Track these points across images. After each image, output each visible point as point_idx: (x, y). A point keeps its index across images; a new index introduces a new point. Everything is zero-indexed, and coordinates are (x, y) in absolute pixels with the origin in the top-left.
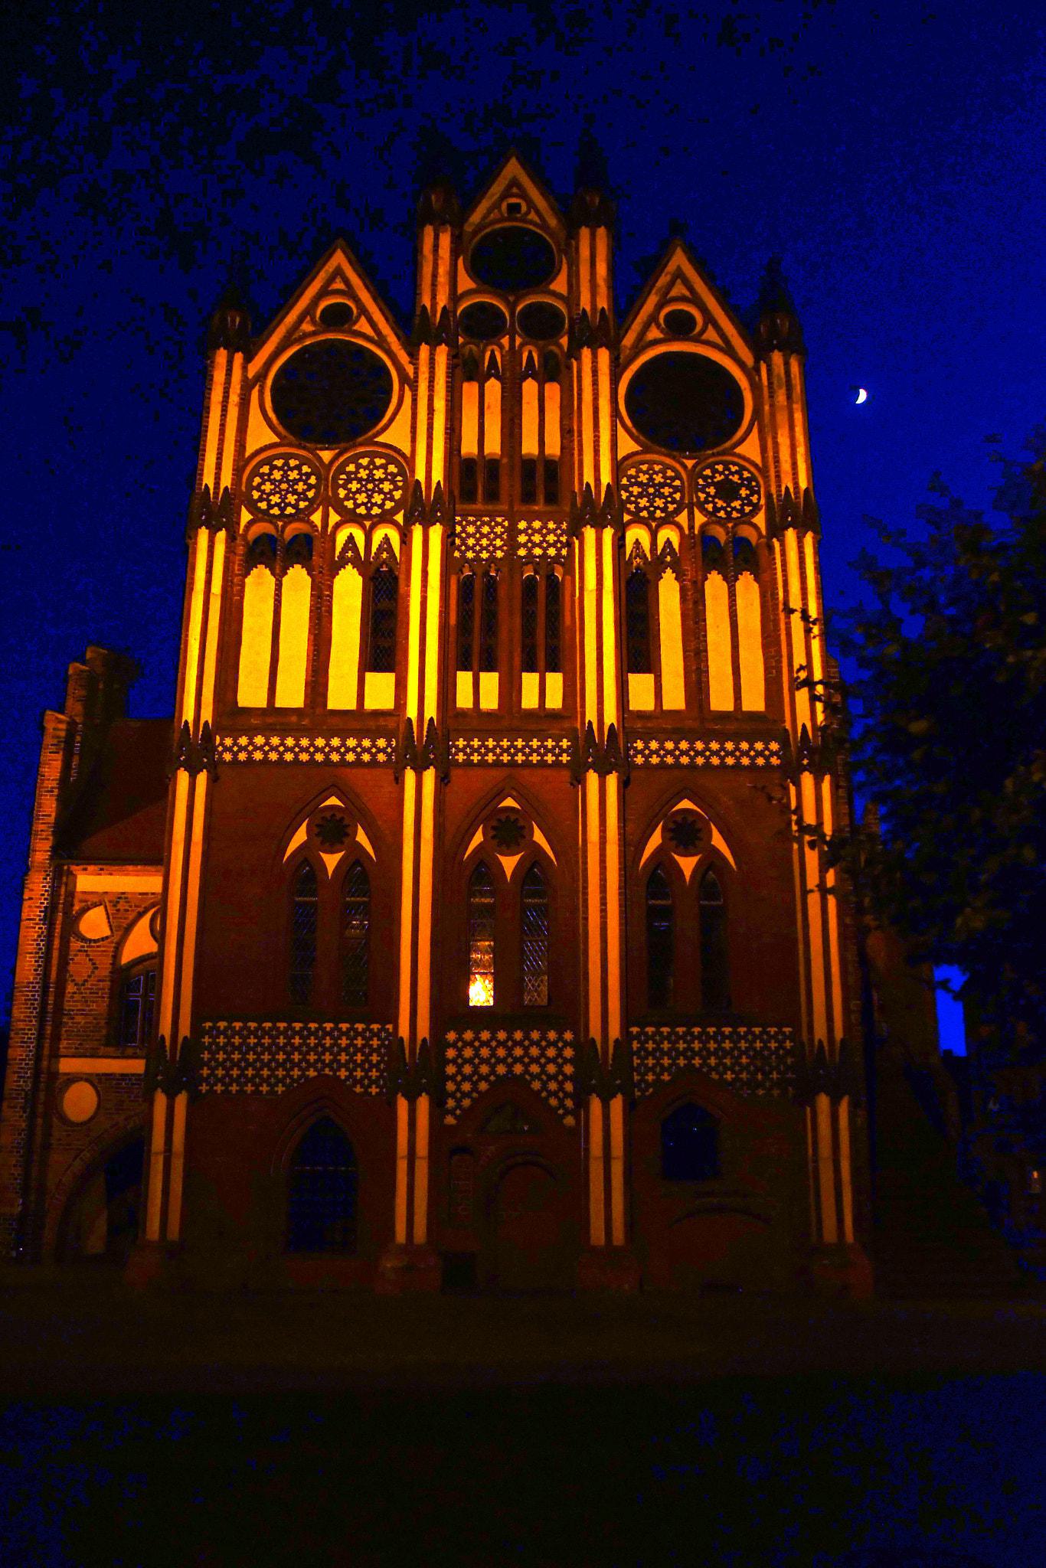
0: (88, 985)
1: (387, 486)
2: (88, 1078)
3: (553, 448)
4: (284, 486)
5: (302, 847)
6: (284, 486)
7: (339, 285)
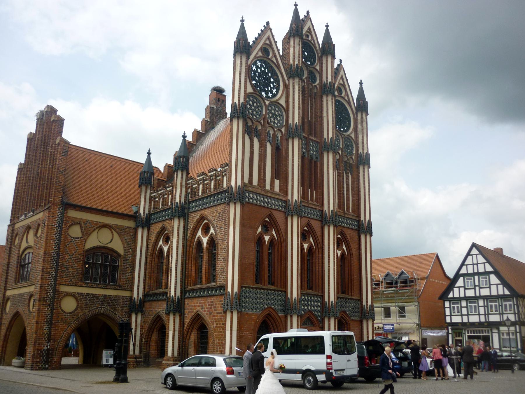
0: (74, 256)
5: (260, 233)
6: (253, 108)
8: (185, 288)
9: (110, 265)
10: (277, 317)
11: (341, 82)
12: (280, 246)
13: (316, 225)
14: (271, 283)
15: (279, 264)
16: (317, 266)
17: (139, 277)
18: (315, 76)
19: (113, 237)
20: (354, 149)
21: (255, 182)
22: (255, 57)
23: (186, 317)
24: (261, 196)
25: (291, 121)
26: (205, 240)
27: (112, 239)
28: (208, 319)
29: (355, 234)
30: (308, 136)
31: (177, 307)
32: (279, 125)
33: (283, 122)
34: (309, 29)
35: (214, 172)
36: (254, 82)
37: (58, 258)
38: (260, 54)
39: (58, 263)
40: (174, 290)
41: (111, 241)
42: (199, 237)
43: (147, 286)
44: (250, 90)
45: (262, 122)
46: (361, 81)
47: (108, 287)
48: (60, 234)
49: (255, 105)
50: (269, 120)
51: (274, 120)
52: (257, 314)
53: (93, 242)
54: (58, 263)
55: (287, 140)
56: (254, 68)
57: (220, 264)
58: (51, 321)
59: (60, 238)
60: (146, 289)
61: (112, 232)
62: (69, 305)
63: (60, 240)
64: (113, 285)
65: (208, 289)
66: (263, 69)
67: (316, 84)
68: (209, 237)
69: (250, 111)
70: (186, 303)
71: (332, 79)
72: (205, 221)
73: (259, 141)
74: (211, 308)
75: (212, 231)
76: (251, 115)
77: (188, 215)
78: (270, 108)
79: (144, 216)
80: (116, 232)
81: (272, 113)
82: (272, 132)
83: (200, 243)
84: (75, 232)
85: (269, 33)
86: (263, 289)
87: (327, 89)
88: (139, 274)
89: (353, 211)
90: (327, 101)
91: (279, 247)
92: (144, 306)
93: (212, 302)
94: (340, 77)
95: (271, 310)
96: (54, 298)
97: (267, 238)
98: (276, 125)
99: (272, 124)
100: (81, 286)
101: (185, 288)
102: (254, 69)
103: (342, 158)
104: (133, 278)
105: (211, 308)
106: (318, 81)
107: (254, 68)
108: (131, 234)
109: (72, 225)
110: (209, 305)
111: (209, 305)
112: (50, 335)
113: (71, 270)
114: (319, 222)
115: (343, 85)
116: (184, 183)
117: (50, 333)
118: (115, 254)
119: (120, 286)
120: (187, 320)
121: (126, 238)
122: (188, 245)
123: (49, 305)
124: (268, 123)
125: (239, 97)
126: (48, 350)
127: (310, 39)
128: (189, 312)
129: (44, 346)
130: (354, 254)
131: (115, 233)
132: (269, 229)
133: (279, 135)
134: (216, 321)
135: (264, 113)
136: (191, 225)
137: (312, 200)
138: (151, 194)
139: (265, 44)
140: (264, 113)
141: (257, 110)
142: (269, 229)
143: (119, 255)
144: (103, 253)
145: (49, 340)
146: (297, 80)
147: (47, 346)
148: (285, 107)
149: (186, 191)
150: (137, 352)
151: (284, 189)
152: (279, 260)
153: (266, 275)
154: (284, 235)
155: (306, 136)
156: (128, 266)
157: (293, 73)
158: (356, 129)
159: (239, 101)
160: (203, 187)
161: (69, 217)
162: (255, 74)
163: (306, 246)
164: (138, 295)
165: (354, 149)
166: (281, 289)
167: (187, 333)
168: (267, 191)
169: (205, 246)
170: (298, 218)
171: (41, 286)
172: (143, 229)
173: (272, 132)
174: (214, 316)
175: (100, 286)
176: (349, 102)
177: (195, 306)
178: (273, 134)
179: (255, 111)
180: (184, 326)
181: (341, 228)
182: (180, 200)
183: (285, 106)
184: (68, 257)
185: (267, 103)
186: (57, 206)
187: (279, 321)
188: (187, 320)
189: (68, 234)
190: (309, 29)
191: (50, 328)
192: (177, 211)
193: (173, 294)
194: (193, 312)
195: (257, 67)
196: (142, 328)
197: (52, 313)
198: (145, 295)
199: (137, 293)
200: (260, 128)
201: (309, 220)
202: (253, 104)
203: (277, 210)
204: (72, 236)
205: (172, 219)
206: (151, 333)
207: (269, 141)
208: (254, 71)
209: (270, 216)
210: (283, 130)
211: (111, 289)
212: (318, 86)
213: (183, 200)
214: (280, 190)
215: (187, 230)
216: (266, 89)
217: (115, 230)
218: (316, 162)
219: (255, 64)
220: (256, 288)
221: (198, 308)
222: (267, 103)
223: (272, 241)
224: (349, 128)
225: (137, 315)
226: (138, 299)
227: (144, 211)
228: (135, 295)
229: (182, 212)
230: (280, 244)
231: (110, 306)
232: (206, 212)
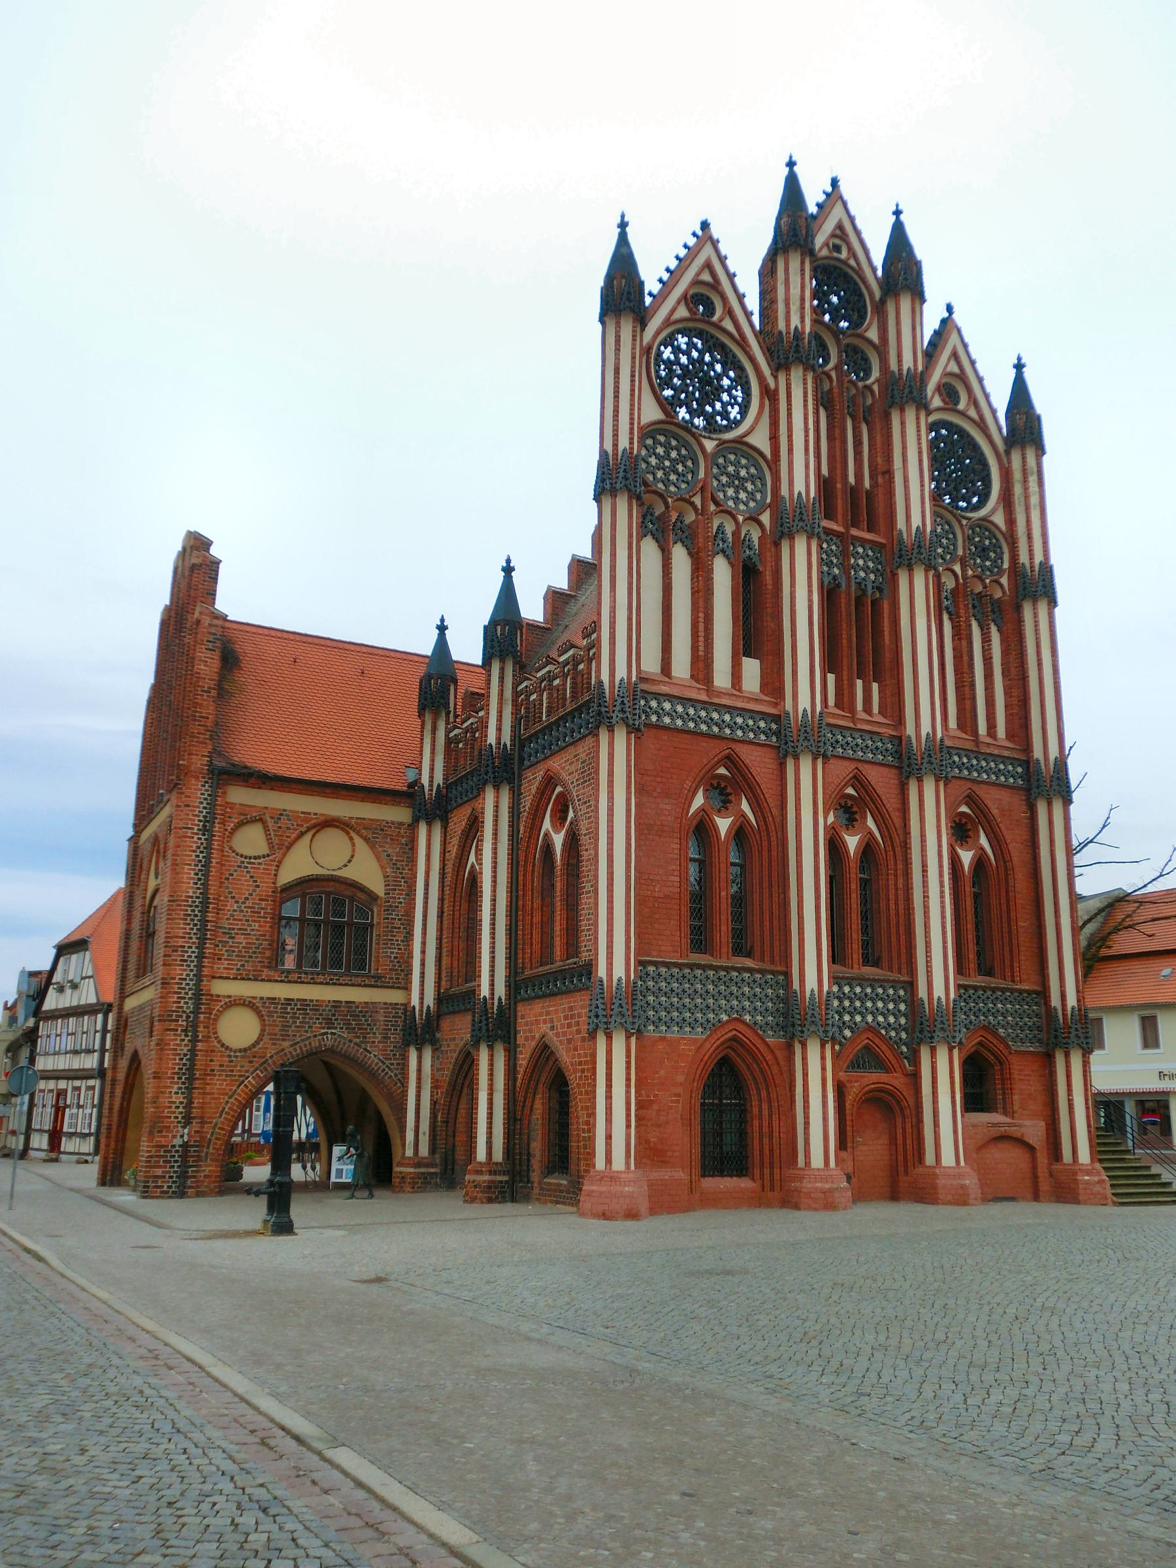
0: (249, 903)
1: (750, 487)
2: (248, 1004)
3: (867, 484)
4: (667, 463)
5: (702, 809)
6: (667, 463)
7: (706, 277)
8: (516, 973)
9: (326, 922)
10: (761, 1047)
11: (953, 368)
12: (765, 843)
13: (881, 780)
14: (740, 949)
15: (766, 895)
16: (892, 896)
17: (423, 952)
18: (866, 360)
19: (354, 851)
20: (1006, 557)
21: (681, 666)
22: (667, 322)
23: (521, 1053)
24: (699, 706)
25: (784, 491)
28: (565, 1057)
29: (1016, 803)
30: (848, 531)
31: (499, 1027)
32: (752, 504)
33: (764, 497)
34: (840, 226)
35: (571, 652)
36: (668, 393)
37: (204, 911)
38: (682, 312)
39: (204, 922)
40: (491, 980)
41: (350, 861)
43: (444, 974)
44: (651, 413)
45: (697, 500)
46: (1019, 359)
47: (346, 979)
48: (209, 847)
49: (674, 454)
50: (721, 495)
51: (737, 492)
52: (695, 1040)
53: (299, 864)
54: (204, 922)
55: (777, 545)
56: (667, 353)
57: (585, 900)
58: (191, 1069)
59: (208, 859)
60: (443, 983)
61: (351, 839)
62: (239, 1030)
63: (207, 865)
64: (357, 976)
65: (561, 974)
66: (695, 354)
67: (868, 382)
68: (567, 832)
69: (660, 474)
70: (519, 1014)
72: (559, 789)
73: (690, 554)
74: (569, 1026)
75: (571, 814)
76: (660, 485)
77: (520, 776)
78: (721, 461)
80: (361, 836)
81: (728, 475)
82: (729, 528)
83: (548, 848)
84: (251, 841)
85: (708, 251)
86: (711, 967)
87: (904, 391)
88: (424, 943)
89: (1010, 735)
90: (903, 423)
91: (763, 845)
92: (438, 1028)
93: (571, 1009)
95: (741, 1027)
96: (196, 1011)
97: (723, 824)
98: (742, 507)
99: (731, 503)
100: (269, 981)
101: (516, 973)
102: (665, 356)
103: (965, 583)
105: (569, 1026)
106: (875, 374)
107: (667, 353)
108: (403, 841)
109: (241, 824)
110: (566, 1018)
111: (566, 1018)
112: (189, 1105)
113: (241, 939)
114: (894, 771)
115: (962, 377)
117: (190, 1102)
118: (360, 894)
119: (378, 977)
120: (523, 1061)
121: (390, 851)
122: (522, 857)
123: (185, 1031)
124: (717, 503)
125: (616, 435)
126: (185, 1145)
127: (844, 255)
128: (527, 1039)
129: (174, 1137)
130: (1015, 860)
131: (358, 841)
132: (732, 798)
133: (755, 535)
134: (580, 1063)
135: (702, 475)
136: (527, 802)
137: (867, 708)
139: (696, 282)
140: (702, 475)
141: (680, 468)
142: (732, 798)
143: (373, 897)
144: (328, 894)
145: (188, 1120)
146: (797, 374)
147: (182, 1136)
148: (769, 457)
150: (424, 1151)
151: (773, 683)
152: (766, 885)
153: (724, 928)
154: (775, 812)
155: (841, 529)
156: (397, 923)
157: (784, 352)
158: (1007, 499)
159: (615, 445)
160: (550, 696)
161: (232, 806)
162: (671, 372)
163: (852, 842)
164: (422, 999)
165: (1006, 557)
166: (772, 968)
167: (525, 1097)
168: (720, 694)
169: (559, 857)
170: (815, 760)
171: (165, 984)
172: (429, 824)
173: (729, 528)
174: (575, 1049)
175: (321, 978)
176: (982, 425)
178: (733, 534)
179: (676, 472)
180: (515, 1080)
181: (969, 785)
182: (499, 739)
183: (767, 452)
184: (231, 906)
185: (710, 445)
186: (197, 778)
187: (769, 1057)
188: (523, 1061)
189: (231, 848)
190: (840, 226)
191: (190, 1090)
192: (490, 769)
193: (485, 991)
194: (533, 1037)
195: (677, 350)
196: (435, 1086)
197: (193, 1051)
198: (439, 999)
199: (422, 992)
200: (690, 517)
201: (860, 766)
202: (667, 454)
203: (751, 743)
204: (241, 851)
205: (480, 790)
206: (455, 1099)
207: (723, 551)
208: (668, 363)
209: (730, 761)
210: (765, 518)
211: (353, 985)
212: (876, 388)
213: (506, 738)
214: (764, 686)
216: (708, 409)
217: (358, 833)
219: (669, 341)
220: (691, 966)
221: (545, 1028)
222: (710, 445)
223: (740, 833)
224: (984, 498)
225: (419, 1050)
226: (421, 1010)
229: (505, 769)
230: (765, 838)
231: (350, 1029)
232: (556, 764)
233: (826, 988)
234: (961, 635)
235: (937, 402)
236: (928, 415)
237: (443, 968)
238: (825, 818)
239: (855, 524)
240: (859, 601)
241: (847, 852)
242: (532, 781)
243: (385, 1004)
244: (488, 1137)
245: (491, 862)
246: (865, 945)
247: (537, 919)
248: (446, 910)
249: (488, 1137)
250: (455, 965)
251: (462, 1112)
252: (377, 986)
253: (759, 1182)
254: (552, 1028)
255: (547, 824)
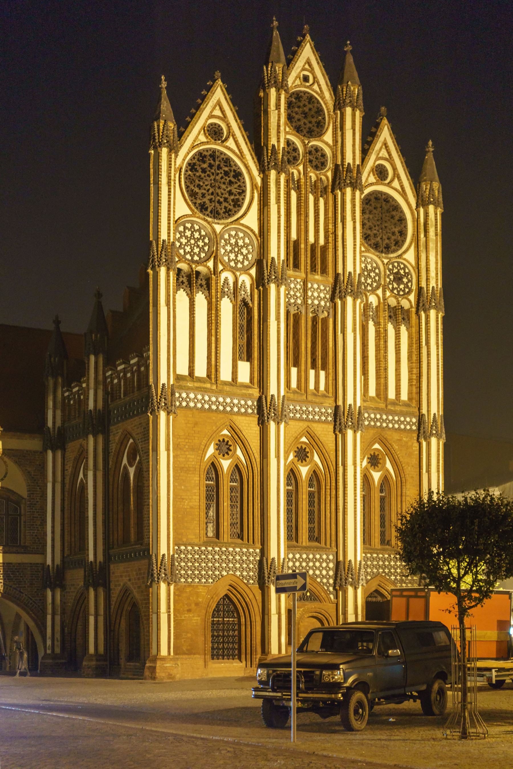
17: (53, 532)
21: (201, 371)
26: (132, 471)
27: (6, 474)
28: (137, 595)
41: (5, 477)
42: (131, 466)
51: (236, 256)
68: (136, 467)
70: (111, 571)
71: (354, 159)
75: (138, 458)
79: (54, 431)
88: (53, 527)
94: (378, 145)
95: (234, 579)
104: (45, 534)
105: (139, 579)
111: (137, 574)
116: (101, 378)
128: (116, 586)
138: (63, 393)
149: (105, 391)
150: (58, 650)
169: (132, 481)
177: (121, 576)
178: (234, 283)
193: (91, 558)
194: (120, 585)
201: (309, 424)
205: (86, 437)
215: (108, 456)
218: (325, 321)
225: (53, 591)
226: (53, 567)
227: (54, 423)
228: (49, 562)
233: (282, 556)
234: (381, 337)
235: (372, 179)
236: (362, 192)
237: (66, 541)
238: (286, 459)
239: (313, 269)
240: (315, 320)
241: (301, 477)
242: (117, 432)
243: (31, 564)
244: (94, 641)
245: (91, 481)
246: (311, 530)
247: (121, 515)
248: (66, 506)
249: (94, 641)
250: (73, 539)
251: (80, 627)
252: (25, 553)
253: (244, 662)
254: (130, 580)
255: (125, 461)
